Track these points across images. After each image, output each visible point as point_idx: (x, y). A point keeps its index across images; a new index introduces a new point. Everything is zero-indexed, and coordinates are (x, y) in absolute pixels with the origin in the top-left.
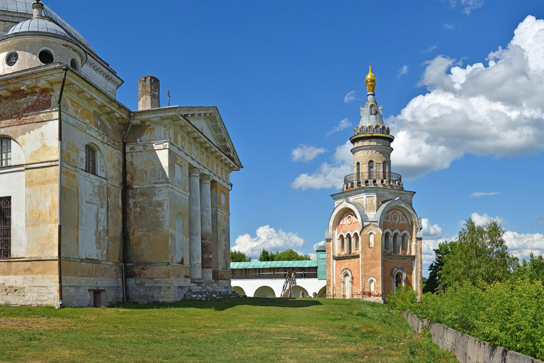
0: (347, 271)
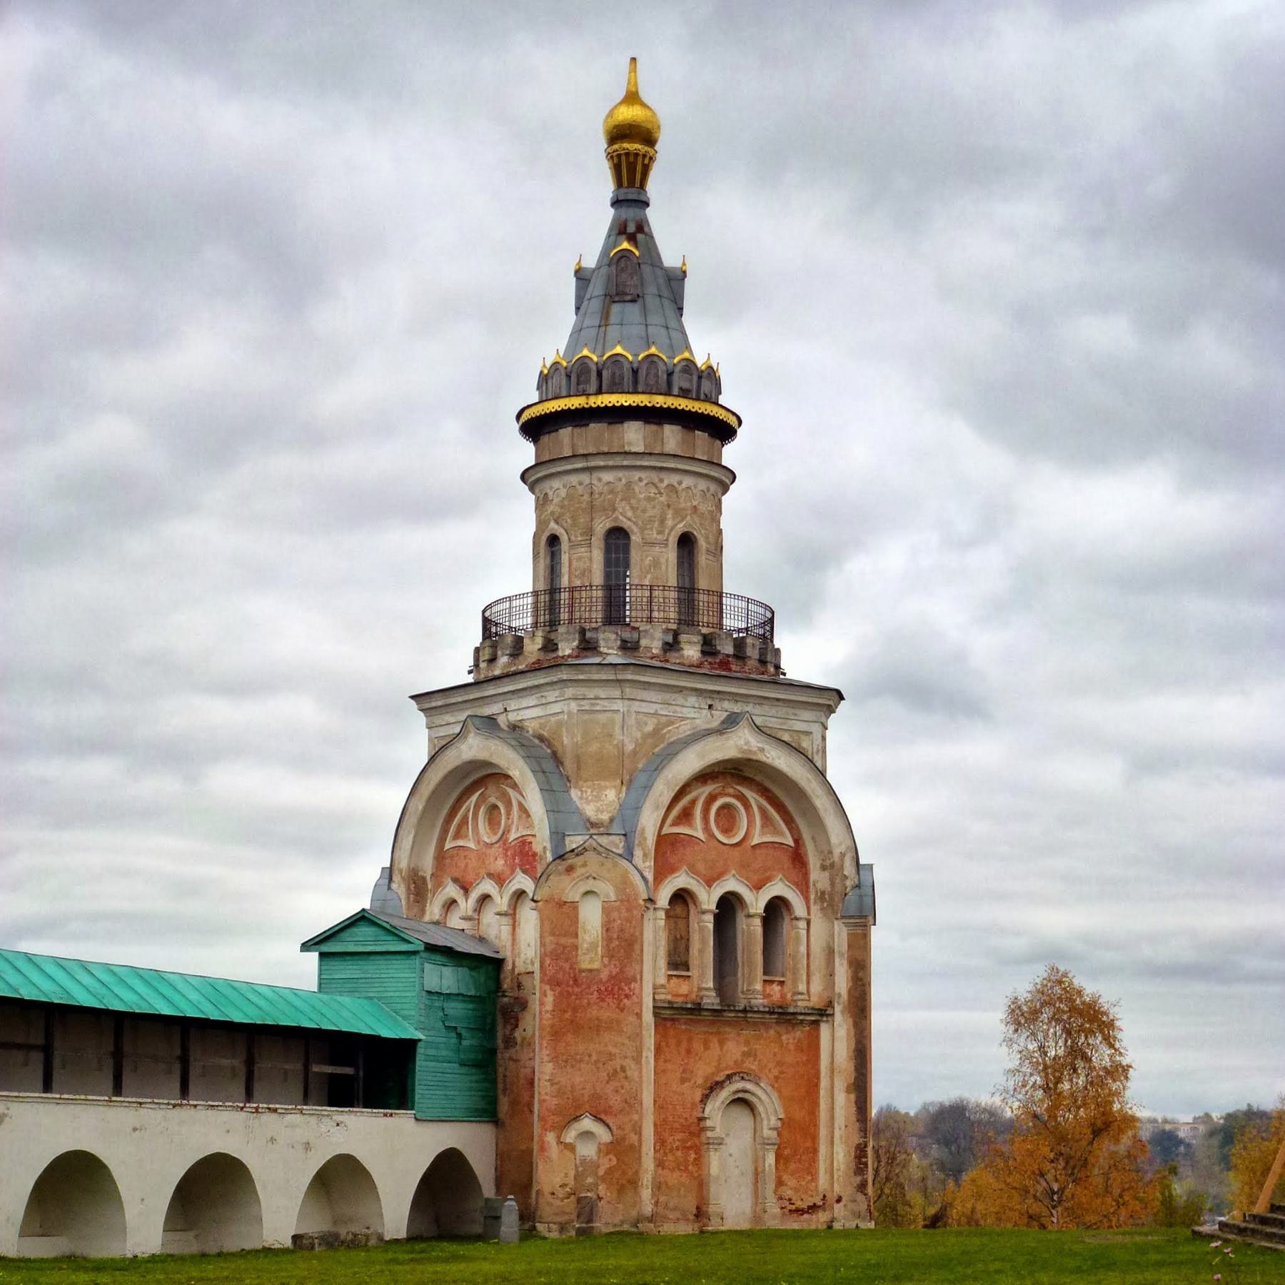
0: (749, 1086)
